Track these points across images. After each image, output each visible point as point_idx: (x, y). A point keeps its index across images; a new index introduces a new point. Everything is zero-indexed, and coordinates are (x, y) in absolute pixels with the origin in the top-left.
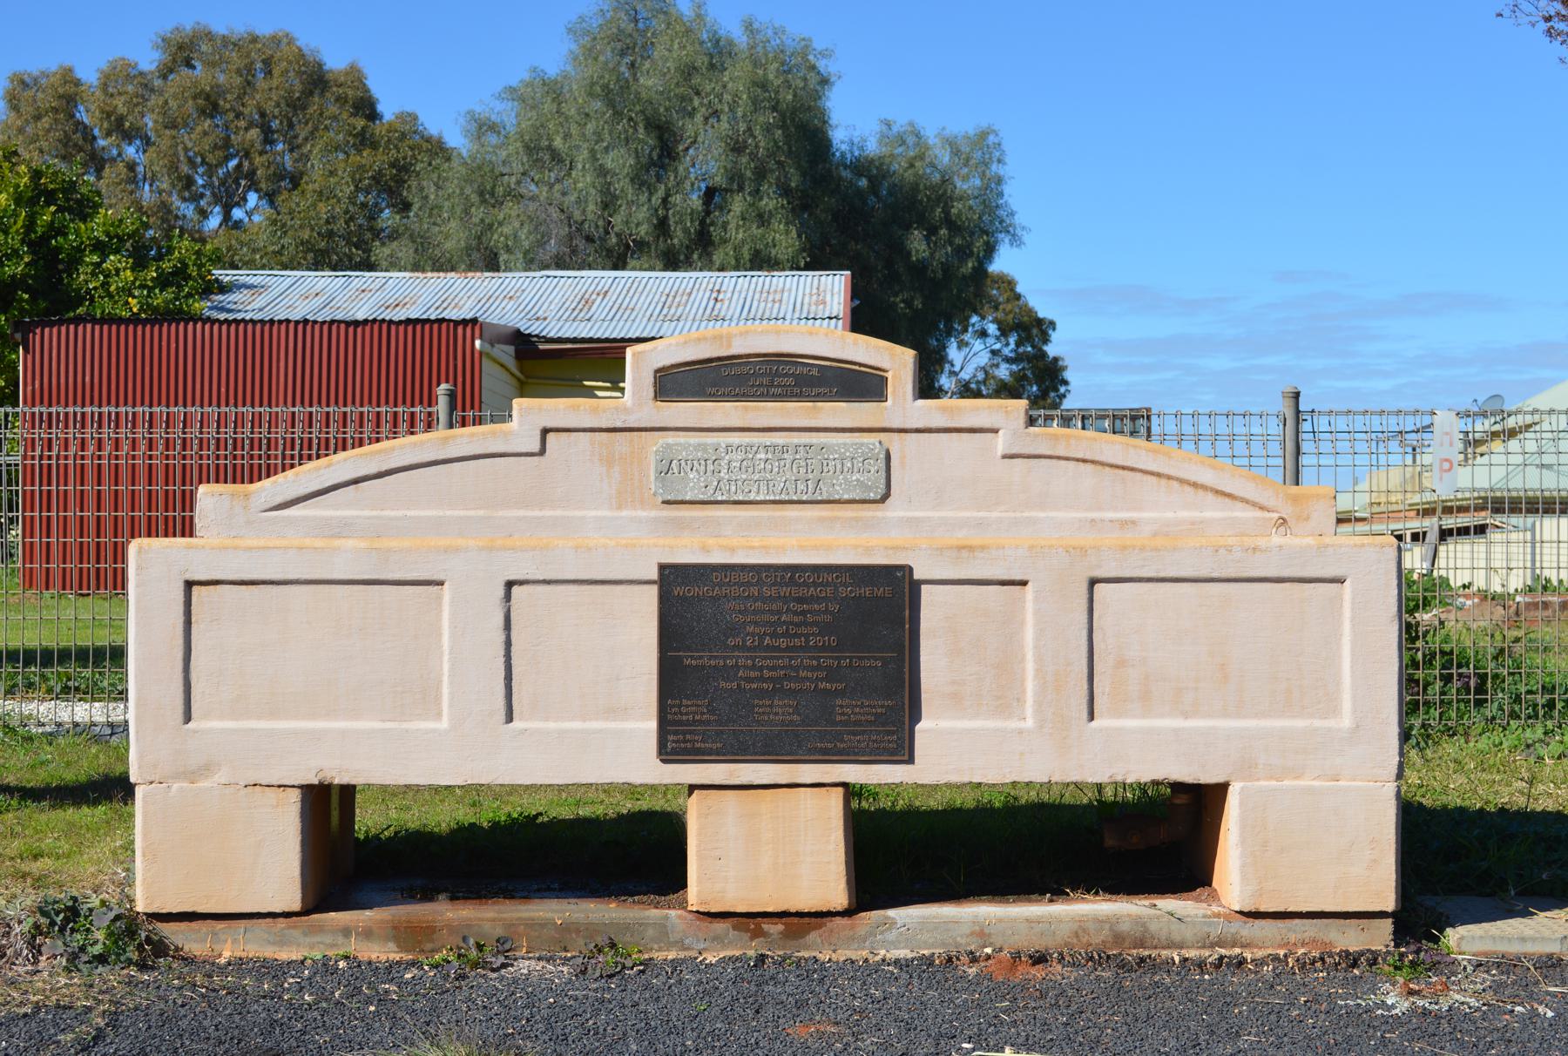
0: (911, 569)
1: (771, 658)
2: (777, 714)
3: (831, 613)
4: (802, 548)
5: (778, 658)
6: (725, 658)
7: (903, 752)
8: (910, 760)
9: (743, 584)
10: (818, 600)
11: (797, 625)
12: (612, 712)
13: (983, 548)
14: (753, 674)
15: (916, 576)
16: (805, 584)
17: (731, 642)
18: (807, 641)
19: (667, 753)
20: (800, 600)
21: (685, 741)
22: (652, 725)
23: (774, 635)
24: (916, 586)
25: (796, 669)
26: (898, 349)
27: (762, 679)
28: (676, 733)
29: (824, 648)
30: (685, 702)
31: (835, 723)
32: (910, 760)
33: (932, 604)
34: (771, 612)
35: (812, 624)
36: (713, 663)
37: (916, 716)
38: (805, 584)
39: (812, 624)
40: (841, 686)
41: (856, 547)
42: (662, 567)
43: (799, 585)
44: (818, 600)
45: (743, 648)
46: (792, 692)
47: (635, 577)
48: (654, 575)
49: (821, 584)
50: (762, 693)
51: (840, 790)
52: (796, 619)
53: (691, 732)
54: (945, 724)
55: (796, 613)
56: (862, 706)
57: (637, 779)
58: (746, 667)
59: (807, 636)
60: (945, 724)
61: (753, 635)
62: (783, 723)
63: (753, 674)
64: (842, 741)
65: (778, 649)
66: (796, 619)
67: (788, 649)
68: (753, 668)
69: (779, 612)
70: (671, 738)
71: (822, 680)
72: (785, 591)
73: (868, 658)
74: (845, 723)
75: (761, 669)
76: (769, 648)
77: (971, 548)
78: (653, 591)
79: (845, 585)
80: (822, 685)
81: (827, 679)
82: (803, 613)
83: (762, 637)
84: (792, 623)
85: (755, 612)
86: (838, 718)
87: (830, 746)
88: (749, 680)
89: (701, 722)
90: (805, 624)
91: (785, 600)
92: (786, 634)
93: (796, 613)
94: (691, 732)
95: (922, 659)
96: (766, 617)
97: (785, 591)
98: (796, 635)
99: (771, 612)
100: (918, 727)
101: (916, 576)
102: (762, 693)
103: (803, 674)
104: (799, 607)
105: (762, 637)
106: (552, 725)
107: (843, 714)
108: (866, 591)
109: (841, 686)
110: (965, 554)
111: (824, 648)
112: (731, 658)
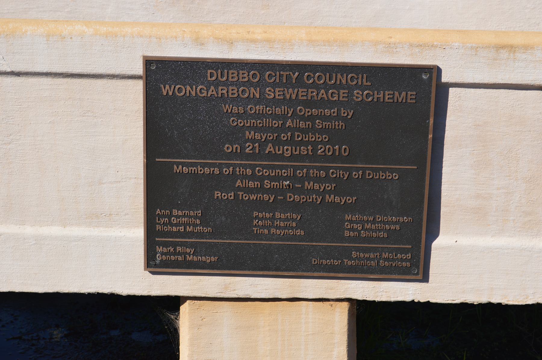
0: (439, 70)
1: (273, 167)
2: (278, 227)
3: (345, 119)
4: (311, 42)
5: (281, 167)
6: (220, 166)
7: (419, 270)
8: (425, 279)
9: (244, 84)
10: (330, 104)
11: (304, 131)
12: (94, 218)
13: (526, 48)
14: (251, 184)
15: (445, 79)
16: (314, 85)
17: (228, 148)
18: (314, 150)
19: (154, 263)
20: (309, 104)
21: (175, 253)
22: (138, 233)
23: (277, 142)
24: (443, 90)
25: (301, 180)
26: (450, 91)
27: (261, 190)
28: (165, 244)
29: (334, 158)
30: (175, 212)
31: (343, 239)
32: (425, 279)
33: (462, 114)
34: (275, 117)
35: (322, 131)
36: (207, 170)
37: (433, 231)
38: (314, 85)
39: (322, 131)
40: (351, 200)
41: (376, 43)
42: (148, 62)
43: (308, 87)
44: (330, 104)
45: (242, 155)
46: (295, 207)
47: (117, 72)
48: (139, 70)
49: (334, 86)
50: (261, 205)
51: (346, 305)
52: (302, 124)
53: (182, 244)
54: (465, 241)
55: (303, 118)
56: (374, 222)
57: (124, 289)
58: (244, 177)
59: (315, 144)
60: (465, 241)
61: (253, 141)
62: (285, 238)
63: (251, 184)
64: (351, 259)
65: (281, 157)
66: (302, 124)
67: (292, 157)
68: (253, 177)
69: (284, 117)
70: (159, 249)
71: (330, 192)
72: (291, 93)
73: (384, 170)
74: (350, 239)
75: (261, 179)
76: (272, 156)
77: (512, 48)
78: (140, 85)
79: (362, 88)
80: (329, 198)
81: (335, 192)
82: (312, 118)
83: (263, 144)
84: (299, 129)
85: (258, 116)
86: (347, 234)
87: (336, 263)
88: (250, 191)
89: (191, 235)
90: (313, 130)
91: (291, 103)
92: (291, 142)
93: (303, 118)
94: (182, 244)
95: (445, 170)
96: (268, 122)
97: (291, 93)
98: (302, 143)
99: (275, 117)
100: (435, 244)
101: (445, 79)
102: (261, 205)
103: (308, 185)
104: (308, 112)
105: (263, 144)
106: (28, 230)
107: (352, 230)
108: (386, 96)
109: (351, 200)
110: (504, 54)
111: (334, 158)
112: (228, 166)
